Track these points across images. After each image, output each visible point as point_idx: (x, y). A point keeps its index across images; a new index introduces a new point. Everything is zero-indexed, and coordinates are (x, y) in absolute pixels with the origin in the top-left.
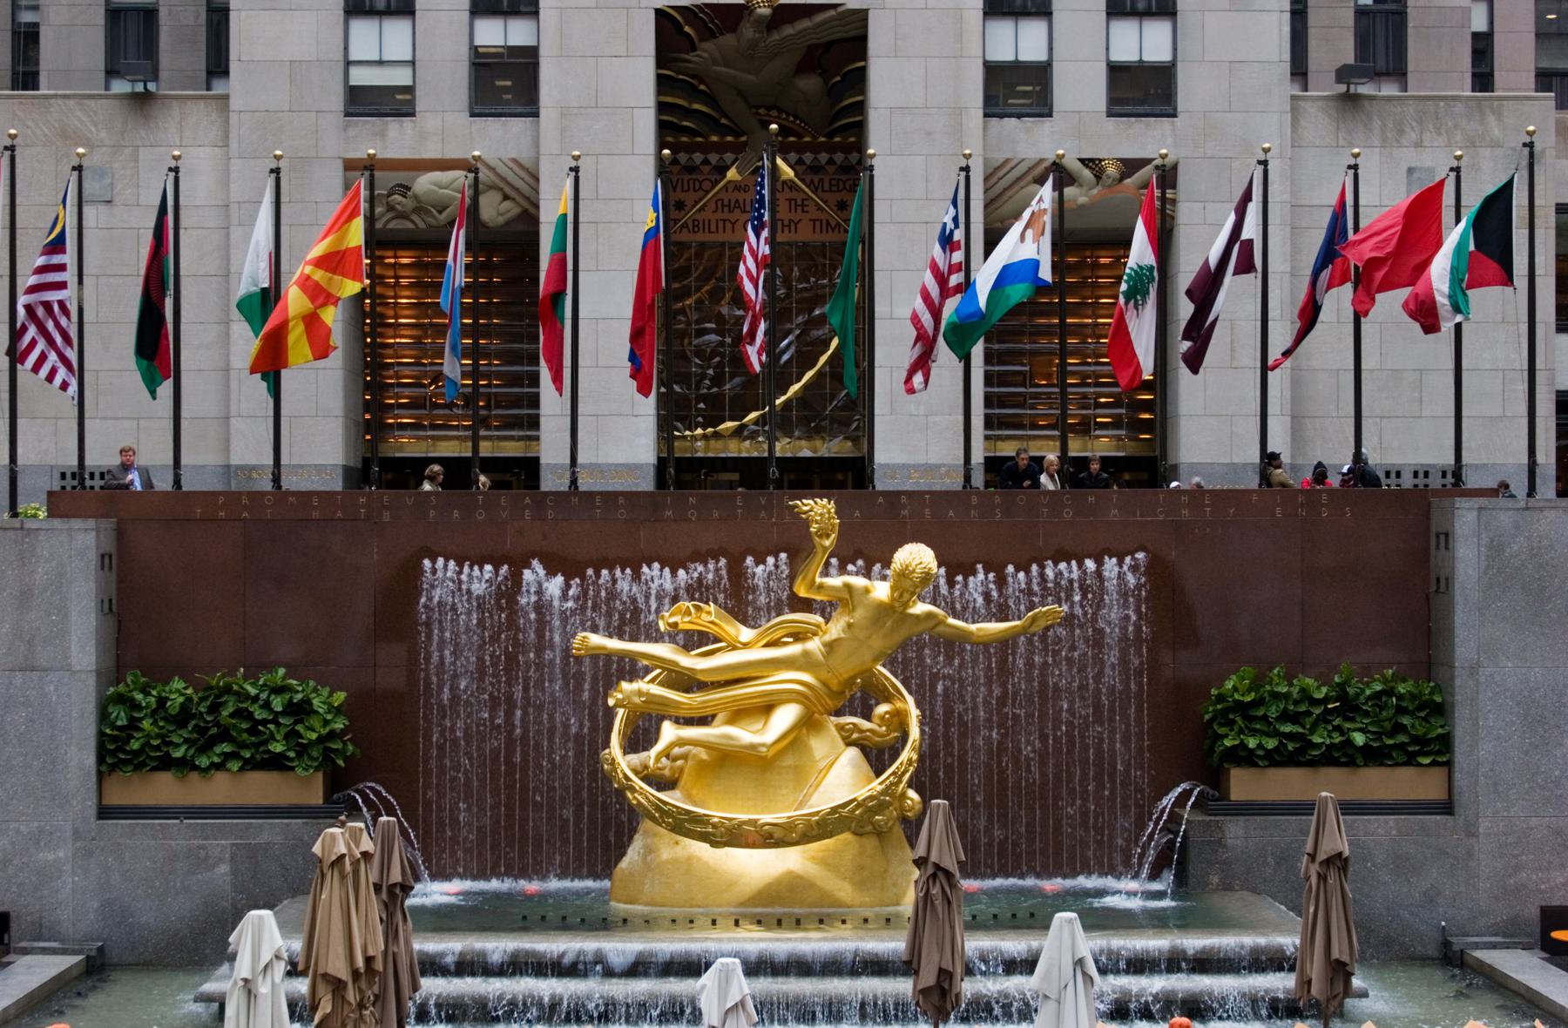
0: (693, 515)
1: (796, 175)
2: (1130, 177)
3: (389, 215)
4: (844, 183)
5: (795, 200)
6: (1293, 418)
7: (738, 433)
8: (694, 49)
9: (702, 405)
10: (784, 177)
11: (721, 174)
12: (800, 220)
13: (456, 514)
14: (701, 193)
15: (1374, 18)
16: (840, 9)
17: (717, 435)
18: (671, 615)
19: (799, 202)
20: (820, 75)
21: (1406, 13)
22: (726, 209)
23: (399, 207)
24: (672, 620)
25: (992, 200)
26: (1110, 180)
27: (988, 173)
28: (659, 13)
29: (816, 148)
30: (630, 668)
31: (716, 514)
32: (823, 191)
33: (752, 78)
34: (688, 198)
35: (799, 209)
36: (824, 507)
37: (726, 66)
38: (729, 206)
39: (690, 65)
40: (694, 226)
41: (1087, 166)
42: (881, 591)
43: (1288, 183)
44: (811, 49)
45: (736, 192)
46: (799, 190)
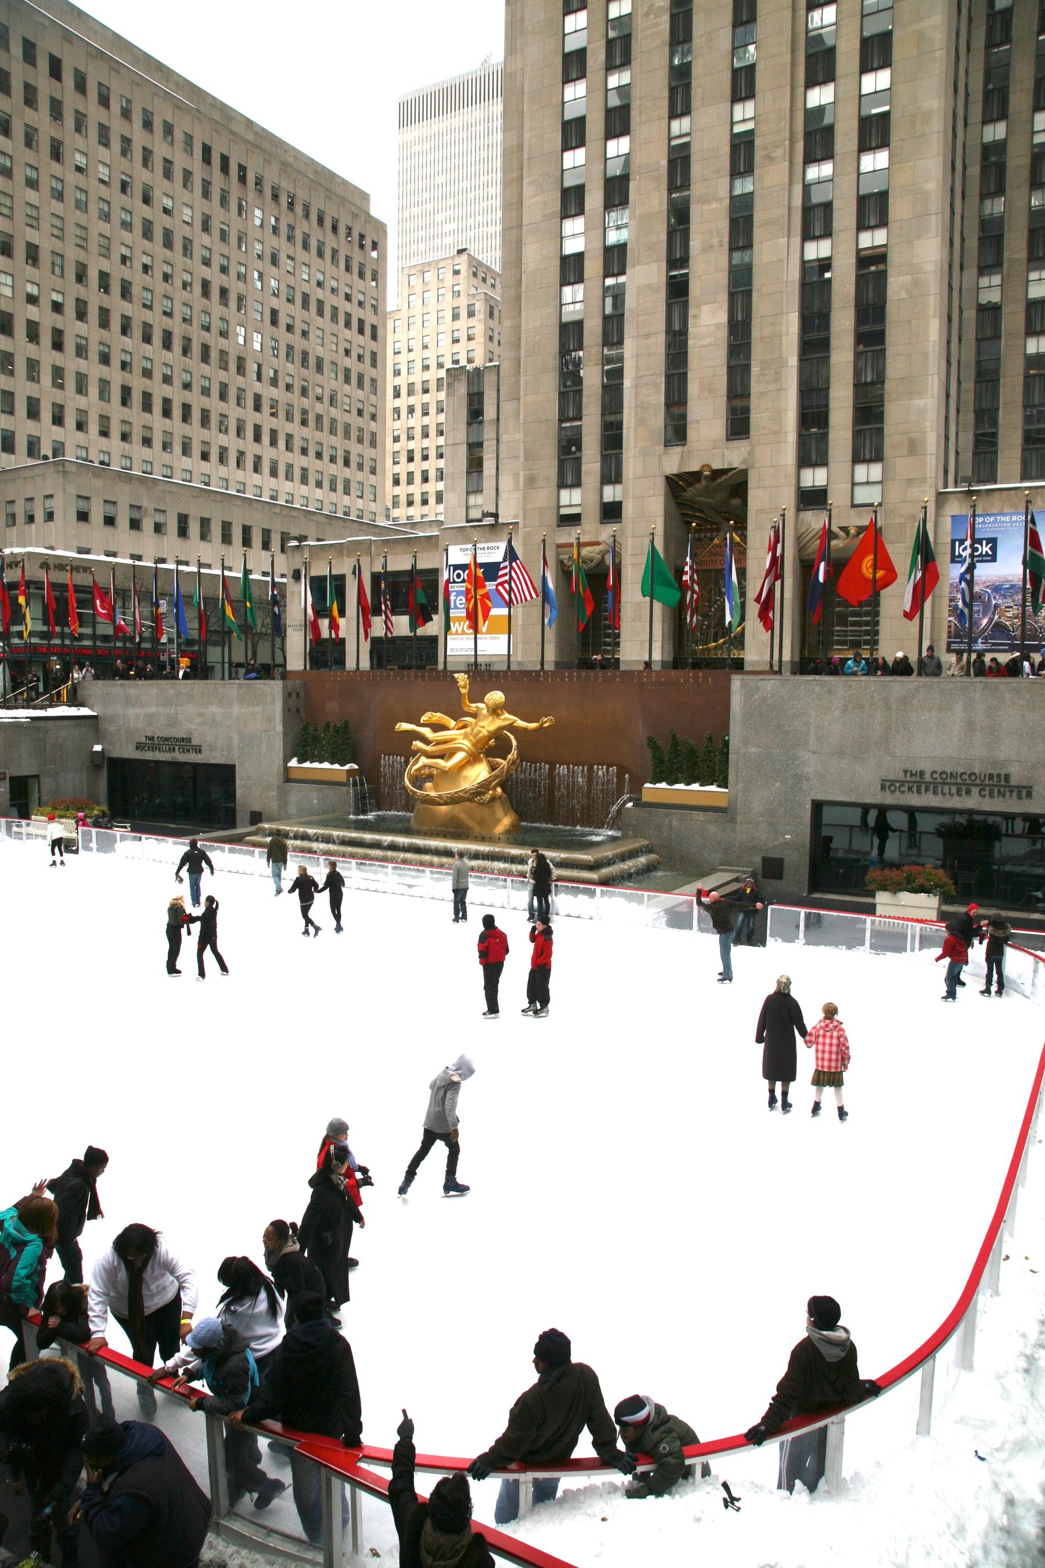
8: (685, 491)
28: (667, 477)
33: (711, 501)
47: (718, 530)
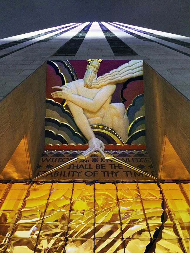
4: (141, 159)
5: (115, 165)
12: (118, 172)
20: (123, 103)
22: (75, 168)
32: (129, 161)
40: (55, 174)
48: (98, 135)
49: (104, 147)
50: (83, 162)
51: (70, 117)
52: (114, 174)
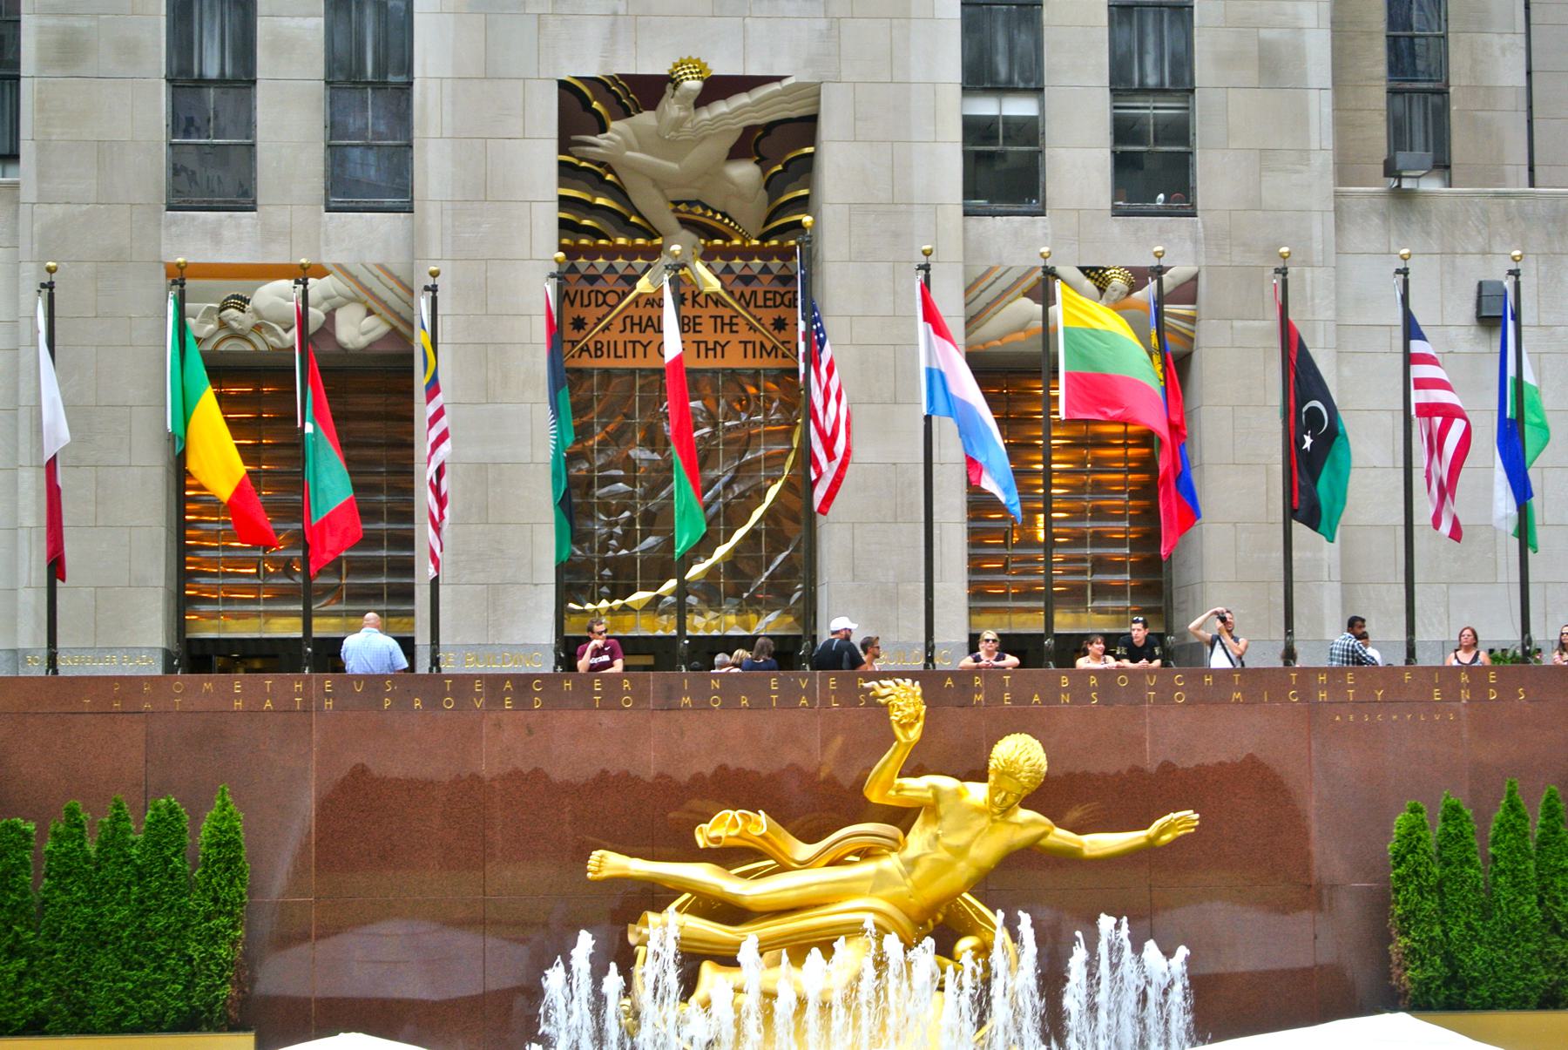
0: (716, 701)
1: (723, 287)
2: (1140, 289)
3: (222, 334)
4: (782, 296)
5: (722, 317)
6: (1343, 583)
7: (654, 605)
8: (603, 129)
9: (607, 572)
10: (707, 290)
11: (630, 285)
13: (417, 704)
14: (605, 309)
15: (1411, 100)
16: (786, 82)
17: (626, 609)
18: (711, 829)
19: (727, 320)
20: (757, 163)
21: (1448, 93)
22: (636, 328)
23: (235, 325)
24: (713, 834)
25: (972, 317)
26: (1117, 293)
27: (970, 282)
28: (563, 85)
29: (747, 254)
30: (656, 896)
31: (744, 701)
32: (756, 306)
33: (674, 166)
34: (590, 314)
35: (727, 328)
36: (906, 689)
37: (642, 150)
38: (640, 324)
39: (600, 150)
40: (596, 349)
41: (1088, 276)
42: (977, 793)
43: (1333, 298)
44: (749, 131)
45: (648, 306)
46: (726, 305)
47: (653, 253)
48: (685, 223)
49: (701, 250)
50: (652, 306)
51: (618, 191)
52: (719, 349)
